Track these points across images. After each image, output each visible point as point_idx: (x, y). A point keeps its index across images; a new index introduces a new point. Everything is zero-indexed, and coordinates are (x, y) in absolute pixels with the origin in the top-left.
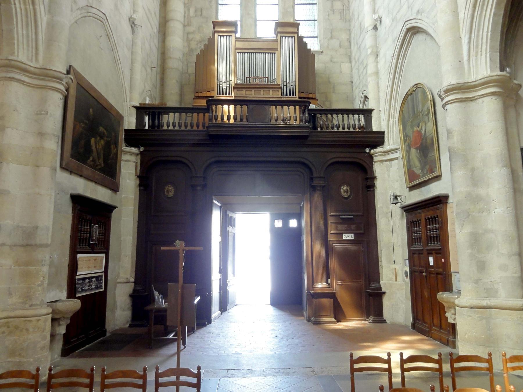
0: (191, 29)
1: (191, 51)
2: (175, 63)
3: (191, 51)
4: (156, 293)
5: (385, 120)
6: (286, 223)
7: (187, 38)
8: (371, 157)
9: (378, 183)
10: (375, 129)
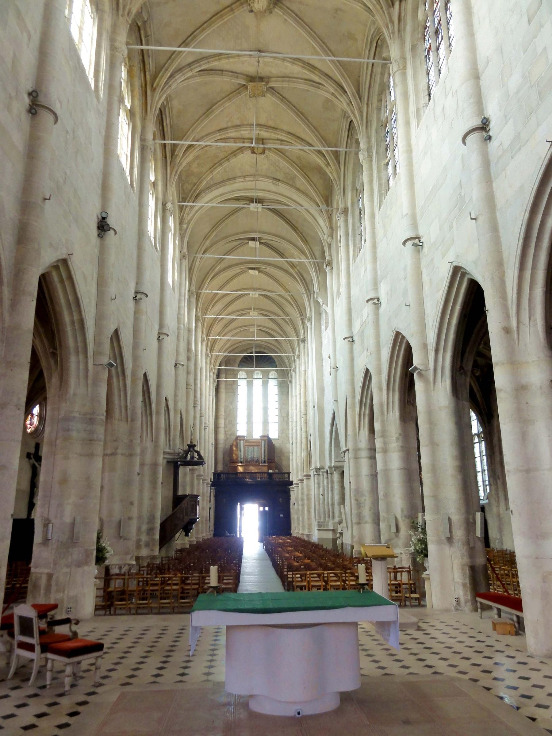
0: (227, 429)
2: (221, 446)
5: (294, 478)
6: (264, 509)
7: (226, 434)
8: (289, 489)
9: (291, 498)
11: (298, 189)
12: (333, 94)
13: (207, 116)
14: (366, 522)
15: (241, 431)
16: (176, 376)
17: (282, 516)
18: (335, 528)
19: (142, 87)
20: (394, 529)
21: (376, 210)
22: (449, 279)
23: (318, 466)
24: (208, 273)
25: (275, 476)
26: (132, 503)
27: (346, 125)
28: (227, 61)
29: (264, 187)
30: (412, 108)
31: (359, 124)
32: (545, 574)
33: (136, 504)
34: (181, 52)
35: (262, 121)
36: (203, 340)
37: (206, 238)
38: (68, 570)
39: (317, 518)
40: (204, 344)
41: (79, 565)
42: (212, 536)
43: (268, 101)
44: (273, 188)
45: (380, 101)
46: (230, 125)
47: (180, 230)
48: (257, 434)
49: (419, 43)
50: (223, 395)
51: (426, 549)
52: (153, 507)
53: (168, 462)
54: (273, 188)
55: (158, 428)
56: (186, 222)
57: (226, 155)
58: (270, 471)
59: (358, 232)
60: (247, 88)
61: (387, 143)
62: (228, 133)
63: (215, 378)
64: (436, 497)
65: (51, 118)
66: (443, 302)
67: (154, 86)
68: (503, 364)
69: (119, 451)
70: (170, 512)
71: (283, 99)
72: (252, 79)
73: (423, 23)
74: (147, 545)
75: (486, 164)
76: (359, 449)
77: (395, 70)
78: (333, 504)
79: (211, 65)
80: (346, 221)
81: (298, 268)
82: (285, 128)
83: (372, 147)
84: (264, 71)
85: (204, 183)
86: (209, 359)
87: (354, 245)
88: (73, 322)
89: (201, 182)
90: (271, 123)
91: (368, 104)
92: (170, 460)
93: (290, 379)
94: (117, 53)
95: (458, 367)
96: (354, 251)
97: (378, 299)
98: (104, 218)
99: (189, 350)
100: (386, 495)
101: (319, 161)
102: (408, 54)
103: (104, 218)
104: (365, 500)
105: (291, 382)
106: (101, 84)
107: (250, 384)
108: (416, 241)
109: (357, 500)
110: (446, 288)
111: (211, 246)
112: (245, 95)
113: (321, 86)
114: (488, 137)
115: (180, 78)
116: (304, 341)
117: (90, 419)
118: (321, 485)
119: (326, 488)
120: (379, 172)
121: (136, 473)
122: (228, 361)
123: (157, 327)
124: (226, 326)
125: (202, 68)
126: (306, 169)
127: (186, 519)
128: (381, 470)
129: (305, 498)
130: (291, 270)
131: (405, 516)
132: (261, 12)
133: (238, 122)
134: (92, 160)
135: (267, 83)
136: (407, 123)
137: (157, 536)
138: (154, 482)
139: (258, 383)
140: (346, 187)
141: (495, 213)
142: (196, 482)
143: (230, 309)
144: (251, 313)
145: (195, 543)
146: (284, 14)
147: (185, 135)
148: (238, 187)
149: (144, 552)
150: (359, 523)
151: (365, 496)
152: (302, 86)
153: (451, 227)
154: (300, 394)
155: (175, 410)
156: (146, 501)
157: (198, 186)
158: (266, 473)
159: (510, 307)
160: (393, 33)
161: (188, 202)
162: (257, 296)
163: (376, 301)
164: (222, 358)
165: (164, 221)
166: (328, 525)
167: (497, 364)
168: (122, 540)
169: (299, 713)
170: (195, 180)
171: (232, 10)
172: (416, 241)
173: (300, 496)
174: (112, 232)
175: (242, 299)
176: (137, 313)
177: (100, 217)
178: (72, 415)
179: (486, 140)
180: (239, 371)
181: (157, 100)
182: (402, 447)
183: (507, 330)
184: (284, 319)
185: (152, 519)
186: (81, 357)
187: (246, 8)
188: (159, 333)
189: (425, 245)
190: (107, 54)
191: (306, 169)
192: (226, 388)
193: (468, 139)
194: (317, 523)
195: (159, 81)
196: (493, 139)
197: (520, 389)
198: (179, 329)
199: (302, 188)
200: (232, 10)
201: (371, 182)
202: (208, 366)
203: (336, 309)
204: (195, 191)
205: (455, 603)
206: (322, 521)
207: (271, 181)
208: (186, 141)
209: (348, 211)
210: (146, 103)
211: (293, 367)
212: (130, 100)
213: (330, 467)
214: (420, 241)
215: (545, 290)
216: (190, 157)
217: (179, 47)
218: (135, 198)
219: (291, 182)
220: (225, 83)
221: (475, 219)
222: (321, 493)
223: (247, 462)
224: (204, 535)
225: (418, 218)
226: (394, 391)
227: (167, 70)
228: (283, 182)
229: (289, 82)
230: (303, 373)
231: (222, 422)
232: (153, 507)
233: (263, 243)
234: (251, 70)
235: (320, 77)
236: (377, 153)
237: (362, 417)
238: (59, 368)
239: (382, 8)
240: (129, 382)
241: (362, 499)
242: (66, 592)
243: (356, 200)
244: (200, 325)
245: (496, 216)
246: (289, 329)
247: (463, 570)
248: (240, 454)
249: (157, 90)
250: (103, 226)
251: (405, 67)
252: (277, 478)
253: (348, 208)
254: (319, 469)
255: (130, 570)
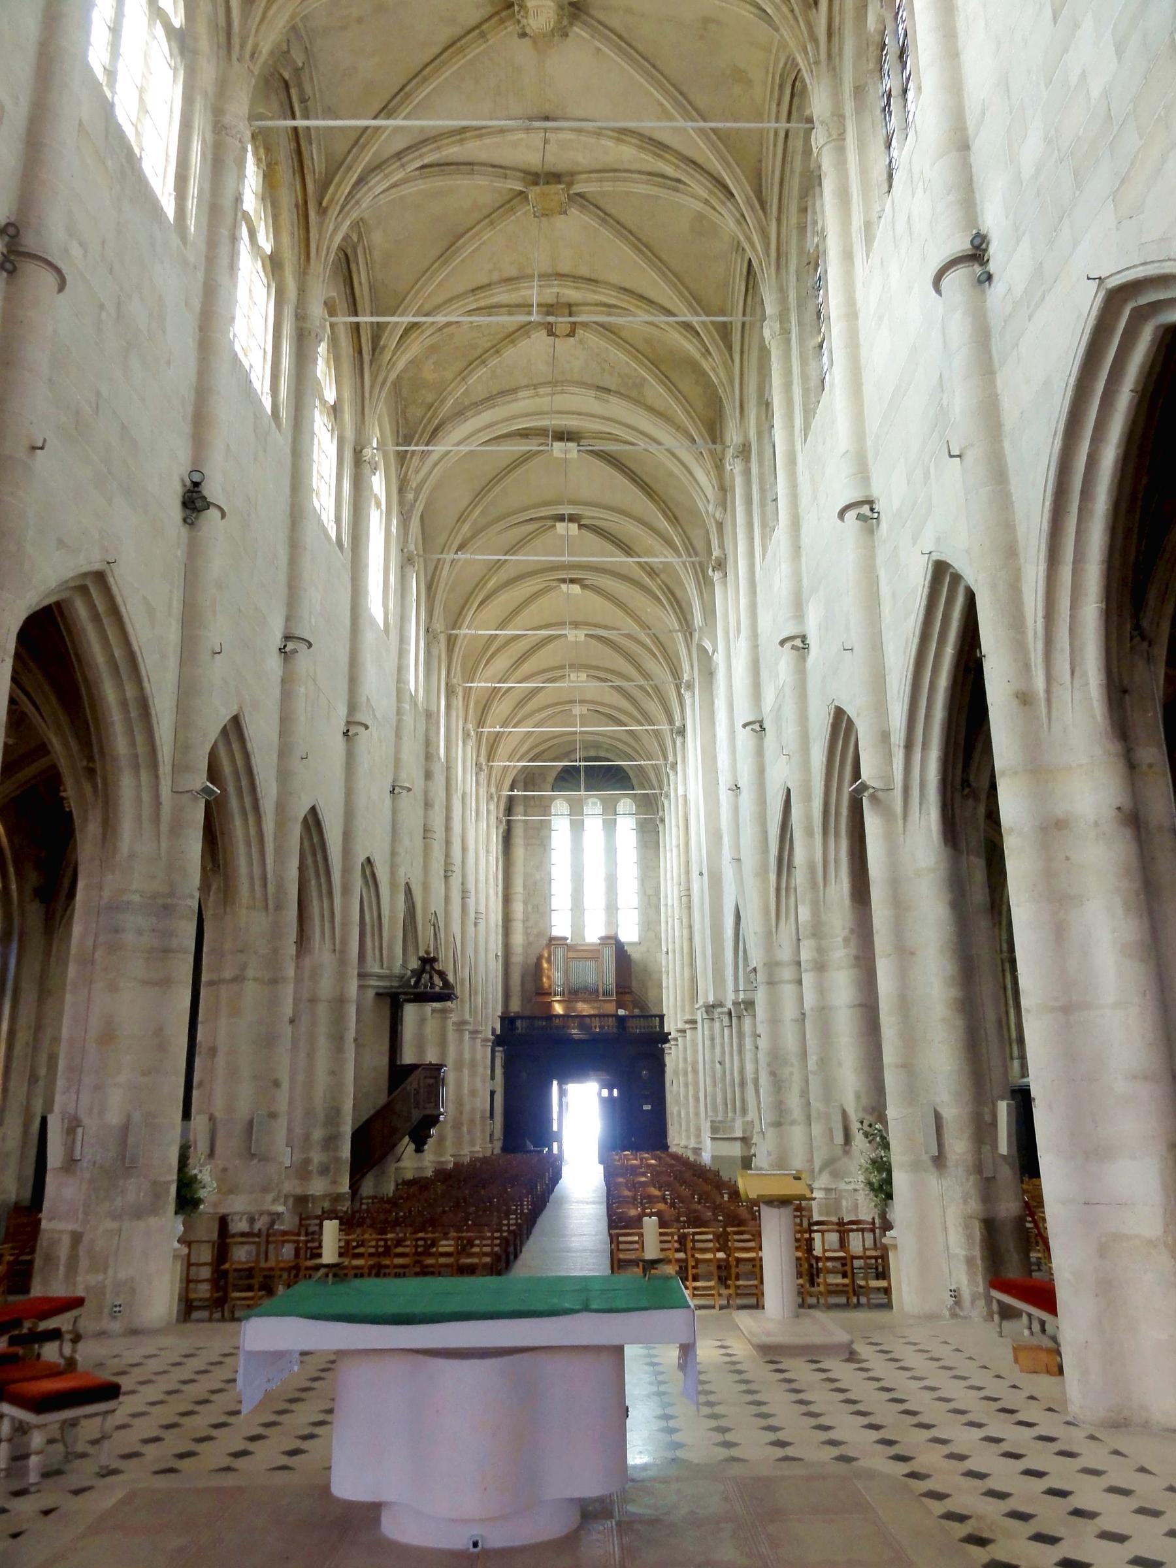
0: (529, 924)
1: (530, 944)
2: (518, 958)
3: (530, 944)
4: (528, 1143)
5: (670, 1026)
6: (611, 1093)
7: (526, 934)
8: (663, 1050)
10: (666, 1031)
11: (651, 409)
12: (706, 202)
13: (445, 262)
14: (792, 1123)
15: (561, 927)
16: (394, 811)
17: (647, 1107)
18: (748, 1134)
19: (297, 206)
20: (839, 1138)
21: (798, 447)
22: (926, 590)
23: (711, 1000)
24: (473, 592)
25: (630, 1023)
26: (277, 1084)
27: (741, 269)
28: (478, 143)
29: (577, 406)
30: (857, 221)
31: (761, 264)
32: (1103, 1240)
33: (285, 1085)
34: (377, 129)
35: (564, 268)
36: (467, 736)
37: (461, 519)
38: (114, 1225)
39: (710, 1113)
40: (472, 743)
41: (139, 1213)
42: (497, 1151)
43: (574, 225)
44: (596, 407)
45: (804, 210)
46: (495, 277)
47: (401, 502)
48: (593, 934)
49: (870, 81)
50: (519, 852)
51: (889, 1181)
52: (336, 1087)
53: (377, 994)
54: (596, 407)
55: (345, 924)
56: (414, 486)
57: (495, 342)
58: (621, 1012)
59: (770, 496)
60: (526, 198)
61: (820, 300)
62: (492, 295)
63: (501, 815)
64: (908, 1067)
65: (50, 279)
66: (916, 640)
67: (324, 204)
68: (1016, 773)
69: (250, 973)
70: (382, 1099)
71: (605, 216)
72: (535, 178)
73: (877, 38)
74: (324, 1171)
75: (982, 336)
76: (778, 964)
77: (821, 142)
78: (743, 1084)
79: (444, 153)
80: (747, 472)
81: (662, 576)
82: (614, 278)
83: (788, 309)
84: (558, 159)
85: (450, 402)
86: (483, 776)
87: (764, 525)
88: (124, 704)
89: (443, 401)
90: (584, 271)
91: (779, 220)
92: (381, 991)
93: (661, 813)
94: (229, 140)
95: (958, 779)
96: (763, 537)
97: (804, 638)
98: (196, 484)
99: (429, 756)
100: (823, 1062)
101: (690, 347)
102: (849, 106)
103: (196, 484)
104: (791, 1074)
105: (662, 820)
106: (191, 204)
107: (577, 827)
108: (865, 509)
109: (773, 1074)
110: (922, 611)
111: (473, 537)
112: (523, 212)
113: (681, 186)
114: (985, 277)
115: (378, 184)
116: (682, 732)
117: (166, 907)
118: (718, 1041)
119: (727, 1049)
120: (804, 362)
121: (286, 1019)
122: (529, 779)
123: (342, 710)
124: (521, 703)
125: (426, 161)
126: (662, 363)
127: (416, 1115)
128: (812, 1009)
129: (690, 1069)
130: (647, 580)
131: (865, 1110)
132: (545, 36)
133: (514, 272)
134: (168, 363)
135: (570, 184)
136: (848, 256)
137: (346, 1151)
138: (338, 1039)
139: (593, 824)
140: (746, 401)
141: (1001, 441)
142: (451, 1035)
143: (526, 668)
144: (573, 676)
145: (451, 1166)
146: (593, 36)
147: (402, 302)
148: (524, 409)
149: (318, 1187)
150: (778, 1124)
151: (792, 1065)
152: (642, 189)
153: (927, 476)
154: (678, 846)
155: (393, 884)
156: (322, 1078)
157: (436, 409)
158: (612, 1016)
159: (1031, 646)
160: (817, 63)
161: (416, 445)
162: (582, 638)
163: (798, 642)
164: (515, 772)
165: (359, 484)
166: (732, 1129)
167: (1003, 773)
168: (256, 1161)
169: (475, 1545)
170: (430, 398)
171: (483, 35)
172: (864, 510)
173: (681, 1065)
174: (213, 513)
175: (550, 647)
176: (287, 683)
177: (188, 482)
178: (125, 898)
179: (980, 282)
180: (553, 798)
181: (333, 233)
182: (857, 958)
183: (1024, 698)
184: (641, 687)
185: (333, 1116)
186: (144, 776)
187: (512, 28)
188: (348, 723)
189: (883, 517)
190: (204, 141)
191: (662, 363)
192: (526, 837)
193: (945, 282)
194: (709, 1124)
195: (334, 194)
196: (995, 278)
197: (1052, 828)
198: (399, 712)
199: (658, 405)
200: (483, 35)
201: (788, 387)
202: (483, 791)
203: (734, 662)
204: (430, 421)
205: (951, 1301)
206: (720, 1118)
207: (593, 393)
208: (402, 315)
209: (749, 451)
210: (308, 239)
211: (666, 789)
212: (271, 236)
213: (736, 1004)
214: (872, 510)
215: (1104, 606)
216: (415, 348)
217: (375, 118)
218: (281, 441)
219: (634, 394)
220: (478, 190)
221: (959, 456)
222: (718, 1058)
223: (573, 994)
224: (477, 1148)
225: (870, 456)
226: (837, 835)
227: (349, 168)
228: (618, 393)
229: (614, 180)
230: (680, 800)
231: (518, 908)
232: (336, 1087)
233: (584, 526)
234: (532, 159)
235: (677, 167)
236: (800, 323)
237: (783, 893)
238: (100, 801)
239: (792, 11)
240: (269, 827)
241: (785, 1072)
242: (110, 1272)
243: (766, 427)
244: (458, 702)
245: (1002, 448)
246: (653, 707)
247: (966, 1227)
248: (555, 977)
249: (330, 212)
250: (194, 501)
251: (842, 136)
252: (636, 1028)
253: (750, 445)
254: (713, 1006)
255: (273, 1223)
